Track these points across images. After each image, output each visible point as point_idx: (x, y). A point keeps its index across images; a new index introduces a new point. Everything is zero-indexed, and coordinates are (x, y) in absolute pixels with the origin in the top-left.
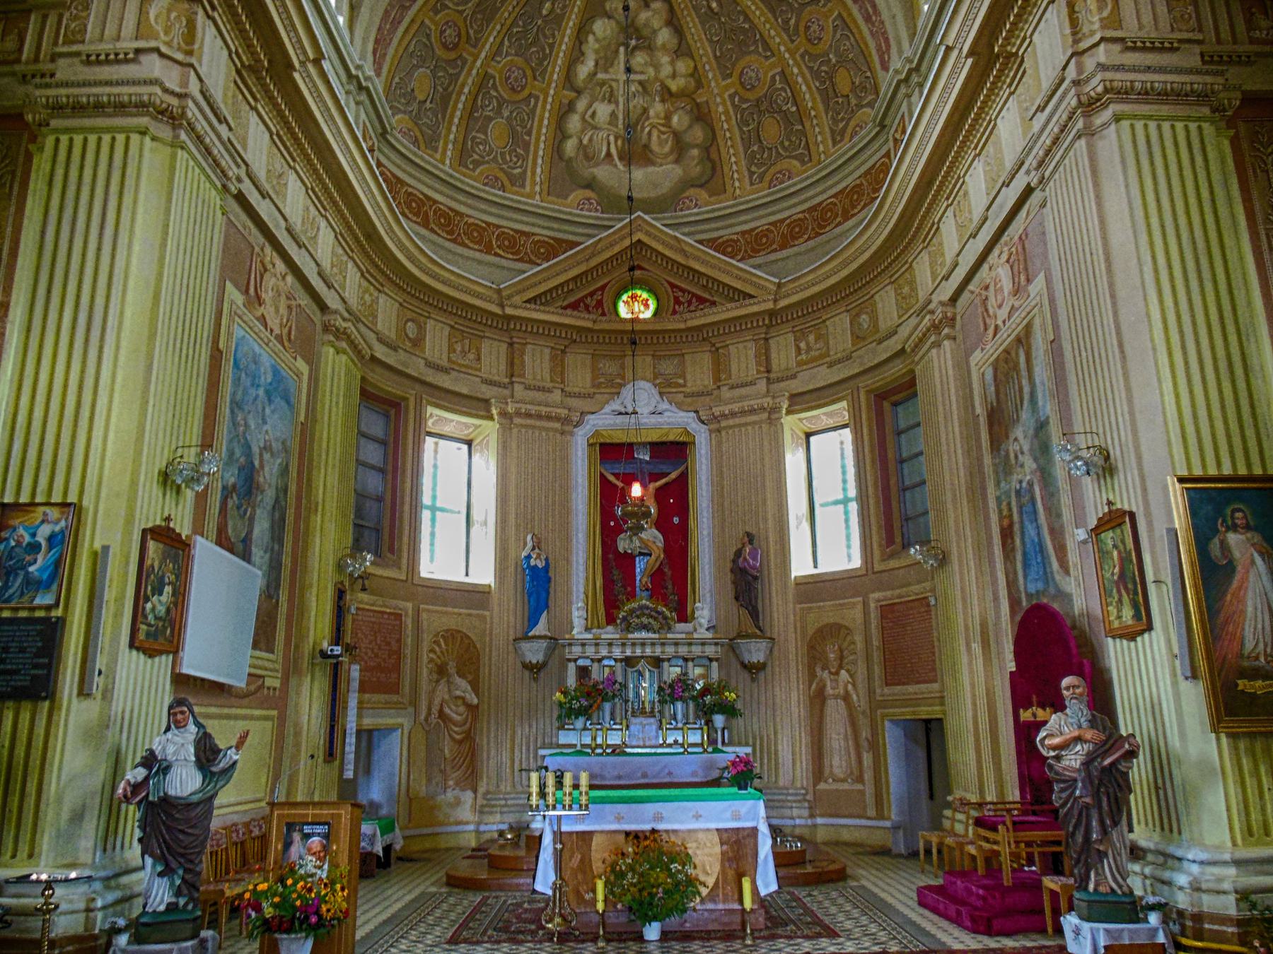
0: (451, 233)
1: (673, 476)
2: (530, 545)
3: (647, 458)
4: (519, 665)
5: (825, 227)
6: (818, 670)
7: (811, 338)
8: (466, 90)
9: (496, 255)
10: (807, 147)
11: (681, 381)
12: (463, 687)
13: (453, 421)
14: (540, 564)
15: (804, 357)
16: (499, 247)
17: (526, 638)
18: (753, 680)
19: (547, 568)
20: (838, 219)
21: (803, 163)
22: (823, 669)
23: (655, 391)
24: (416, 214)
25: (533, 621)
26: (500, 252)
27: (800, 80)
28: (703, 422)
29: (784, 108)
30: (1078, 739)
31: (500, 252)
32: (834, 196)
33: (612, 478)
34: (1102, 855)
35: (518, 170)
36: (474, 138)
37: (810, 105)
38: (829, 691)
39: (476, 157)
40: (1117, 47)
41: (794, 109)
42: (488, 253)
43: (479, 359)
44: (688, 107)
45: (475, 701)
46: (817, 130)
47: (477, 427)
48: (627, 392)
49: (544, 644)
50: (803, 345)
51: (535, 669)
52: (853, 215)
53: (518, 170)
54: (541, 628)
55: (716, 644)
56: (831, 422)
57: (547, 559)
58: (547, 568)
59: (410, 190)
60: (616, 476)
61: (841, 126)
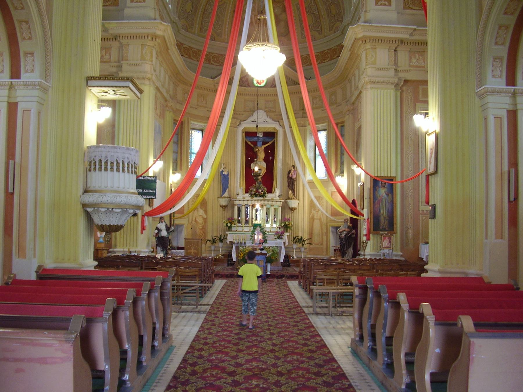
0: (197, 58)
1: (270, 143)
2: (223, 168)
3: (262, 136)
4: (219, 206)
5: (325, 60)
6: (312, 210)
7: (318, 99)
8: (203, 4)
9: (212, 64)
10: (321, 28)
11: (274, 110)
12: (201, 212)
13: (198, 124)
14: (226, 173)
15: (314, 106)
16: (213, 61)
17: (221, 197)
18: (292, 212)
19: (228, 175)
20: (329, 59)
21: (320, 34)
22: (314, 210)
23: (265, 114)
24: (187, 55)
25: (224, 191)
26: (213, 63)
27: (320, 4)
28: (281, 125)
29: (314, 12)
30: (344, 231)
31: (213, 63)
32: (328, 50)
33: (249, 143)
34: (346, 253)
35: (220, 31)
36: (205, 21)
37: (323, 14)
38: (315, 217)
39: (205, 28)
40: (374, 69)
41: (317, 13)
42: (209, 64)
43: (206, 103)
44: (281, 7)
45: (205, 216)
46: (325, 23)
47: (205, 126)
48: (255, 114)
49: (227, 200)
50: (315, 102)
51: (224, 207)
52: (334, 59)
53: (220, 31)
54: (226, 194)
55: (281, 201)
56: (323, 128)
57: (228, 172)
58: (228, 175)
59: (185, 46)
60: (251, 142)
61: (332, 24)
